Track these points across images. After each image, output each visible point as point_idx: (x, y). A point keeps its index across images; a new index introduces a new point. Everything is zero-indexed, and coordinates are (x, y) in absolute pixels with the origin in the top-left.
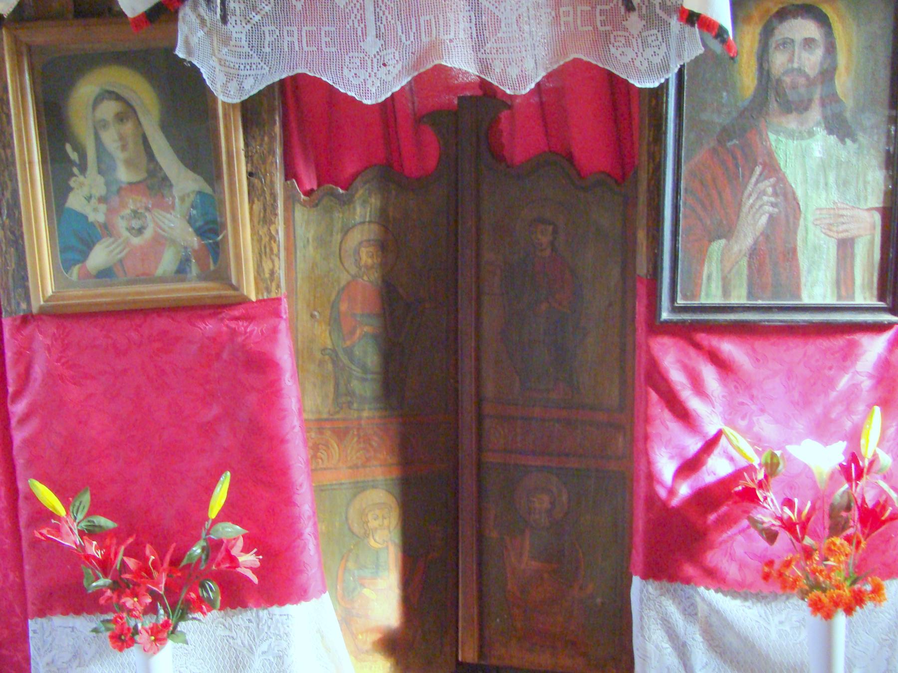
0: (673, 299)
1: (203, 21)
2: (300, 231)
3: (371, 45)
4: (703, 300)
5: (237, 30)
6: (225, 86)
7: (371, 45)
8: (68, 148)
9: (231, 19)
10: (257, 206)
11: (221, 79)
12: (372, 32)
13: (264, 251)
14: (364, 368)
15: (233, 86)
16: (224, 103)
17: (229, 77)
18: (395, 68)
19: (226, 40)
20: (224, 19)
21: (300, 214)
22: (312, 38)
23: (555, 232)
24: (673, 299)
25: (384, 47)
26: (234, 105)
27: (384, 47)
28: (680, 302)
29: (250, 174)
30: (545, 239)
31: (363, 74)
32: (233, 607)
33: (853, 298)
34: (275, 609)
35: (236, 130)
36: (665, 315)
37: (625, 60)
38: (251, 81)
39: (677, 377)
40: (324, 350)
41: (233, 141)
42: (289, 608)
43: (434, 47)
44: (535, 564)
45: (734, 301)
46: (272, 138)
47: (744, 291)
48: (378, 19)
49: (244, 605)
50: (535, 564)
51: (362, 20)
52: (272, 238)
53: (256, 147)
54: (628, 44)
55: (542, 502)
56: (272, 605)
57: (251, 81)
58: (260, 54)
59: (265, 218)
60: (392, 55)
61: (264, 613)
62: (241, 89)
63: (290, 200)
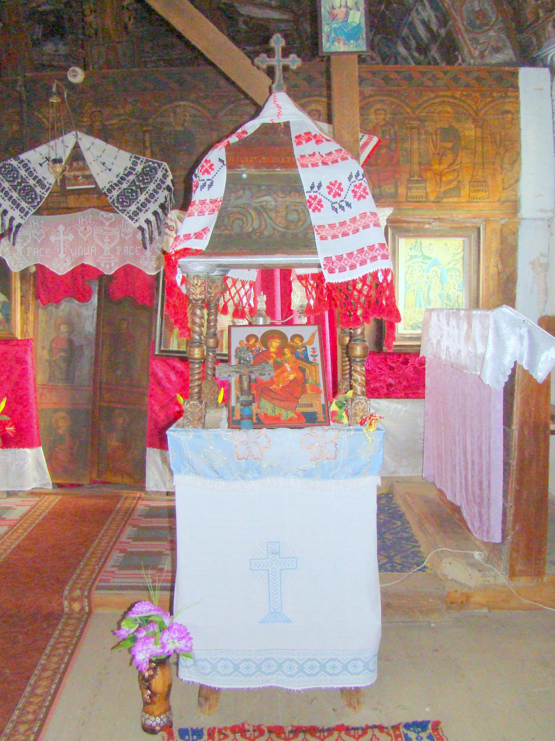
0: (160, 347)
2: (40, 317)
3: (62, 255)
4: (171, 348)
7: (62, 255)
9: (17, 245)
10: (23, 308)
11: (13, 264)
12: (62, 251)
13: (25, 322)
14: (61, 368)
17: (15, 264)
18: (69, 263)
20: (14, 244)
21: (41, 311)
22: (43, 252)
23: (128, 324)
24: (160, 347)
25: (66, 256)
27: (66, 256)
28: (162, 348)
29: (22, 297)
30: (125, 326)
31: (58, 265)
32: (7, 448)
33: (222, 350)
34: (21, 449)
36: (157, 353)
37: (145, 265)
38: (22, 265)
39: (161, 374)
40: (46, 361)
41: (17, 285)
42: (28, 450)
43: (82, 257)
44: (117, 444)
45: (181, 349)
46: (30, 285)
47: (185, 347)
48: (64, 247)
49: (11, 447)
50: (117, 444)
51: (60, 246)
52: (28, 318)
53: (24, 288)
54: (146, 260)
55: (120, 421)
56: (19, 447)
57: (22, 265)
58: (26, 257)
59: (25, 312)
60: (68, 259)
61: (17, 450)
63: (37, 307)
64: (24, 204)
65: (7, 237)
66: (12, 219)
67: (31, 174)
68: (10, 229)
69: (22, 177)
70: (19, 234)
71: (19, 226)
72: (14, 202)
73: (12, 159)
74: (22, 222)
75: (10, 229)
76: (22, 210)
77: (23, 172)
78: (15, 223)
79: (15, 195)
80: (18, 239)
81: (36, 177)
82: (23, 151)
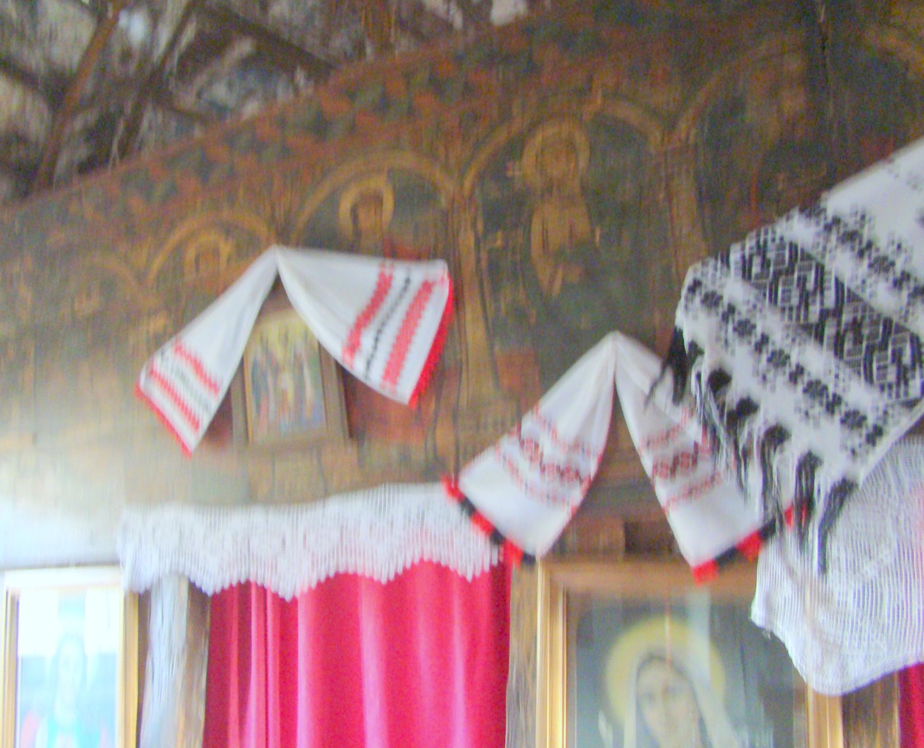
1: (791, 572)
5: (840, 584)
6: (820, 669)
8: (602, 724)
9: (832, 574)
15: (831, 669)
16: (817, 695)
19: (825, 599)
26: (831, 698)
35: (833, 726)
62: (843, 668)
64: (860, 395)
65: (790, 535)
66: (809, 465)
67: (882, 265)
68: (805, 503)
69: (839, 285)
70: (841, 526)
71: (844, 489)
72: (815, 389)
73: (796, 215)
74: (861, 473)
75: (805, 503)
76: (853, 420)
77: (843, 265)
78: (825, 480)
79: (816, 360)
80: (836, 548)
81: (906, 276)
82: (833, 179)
